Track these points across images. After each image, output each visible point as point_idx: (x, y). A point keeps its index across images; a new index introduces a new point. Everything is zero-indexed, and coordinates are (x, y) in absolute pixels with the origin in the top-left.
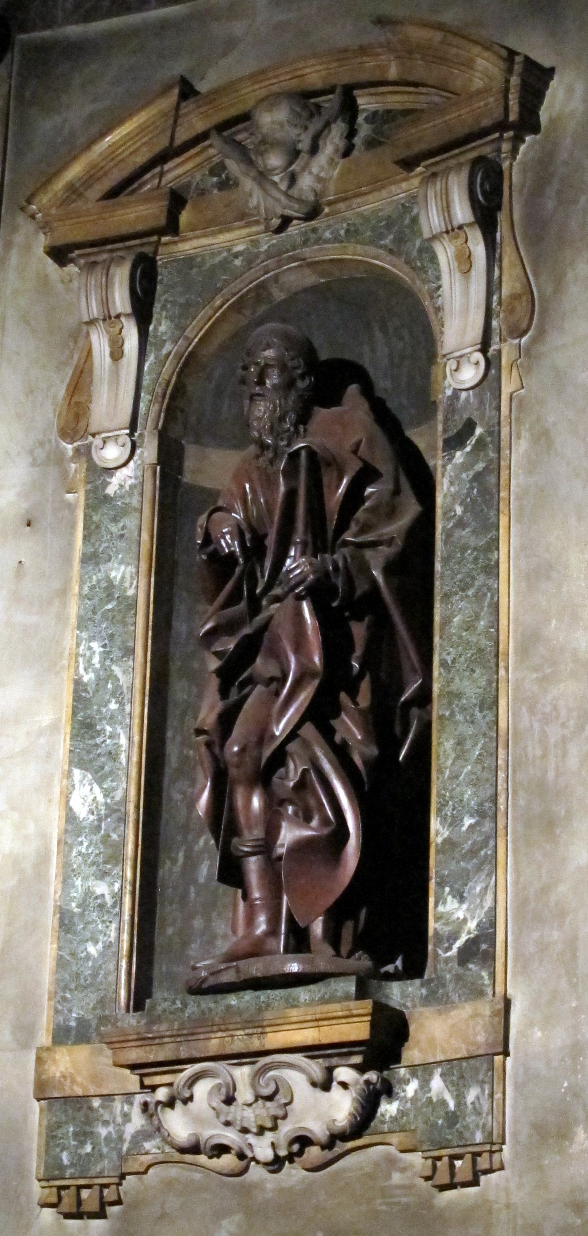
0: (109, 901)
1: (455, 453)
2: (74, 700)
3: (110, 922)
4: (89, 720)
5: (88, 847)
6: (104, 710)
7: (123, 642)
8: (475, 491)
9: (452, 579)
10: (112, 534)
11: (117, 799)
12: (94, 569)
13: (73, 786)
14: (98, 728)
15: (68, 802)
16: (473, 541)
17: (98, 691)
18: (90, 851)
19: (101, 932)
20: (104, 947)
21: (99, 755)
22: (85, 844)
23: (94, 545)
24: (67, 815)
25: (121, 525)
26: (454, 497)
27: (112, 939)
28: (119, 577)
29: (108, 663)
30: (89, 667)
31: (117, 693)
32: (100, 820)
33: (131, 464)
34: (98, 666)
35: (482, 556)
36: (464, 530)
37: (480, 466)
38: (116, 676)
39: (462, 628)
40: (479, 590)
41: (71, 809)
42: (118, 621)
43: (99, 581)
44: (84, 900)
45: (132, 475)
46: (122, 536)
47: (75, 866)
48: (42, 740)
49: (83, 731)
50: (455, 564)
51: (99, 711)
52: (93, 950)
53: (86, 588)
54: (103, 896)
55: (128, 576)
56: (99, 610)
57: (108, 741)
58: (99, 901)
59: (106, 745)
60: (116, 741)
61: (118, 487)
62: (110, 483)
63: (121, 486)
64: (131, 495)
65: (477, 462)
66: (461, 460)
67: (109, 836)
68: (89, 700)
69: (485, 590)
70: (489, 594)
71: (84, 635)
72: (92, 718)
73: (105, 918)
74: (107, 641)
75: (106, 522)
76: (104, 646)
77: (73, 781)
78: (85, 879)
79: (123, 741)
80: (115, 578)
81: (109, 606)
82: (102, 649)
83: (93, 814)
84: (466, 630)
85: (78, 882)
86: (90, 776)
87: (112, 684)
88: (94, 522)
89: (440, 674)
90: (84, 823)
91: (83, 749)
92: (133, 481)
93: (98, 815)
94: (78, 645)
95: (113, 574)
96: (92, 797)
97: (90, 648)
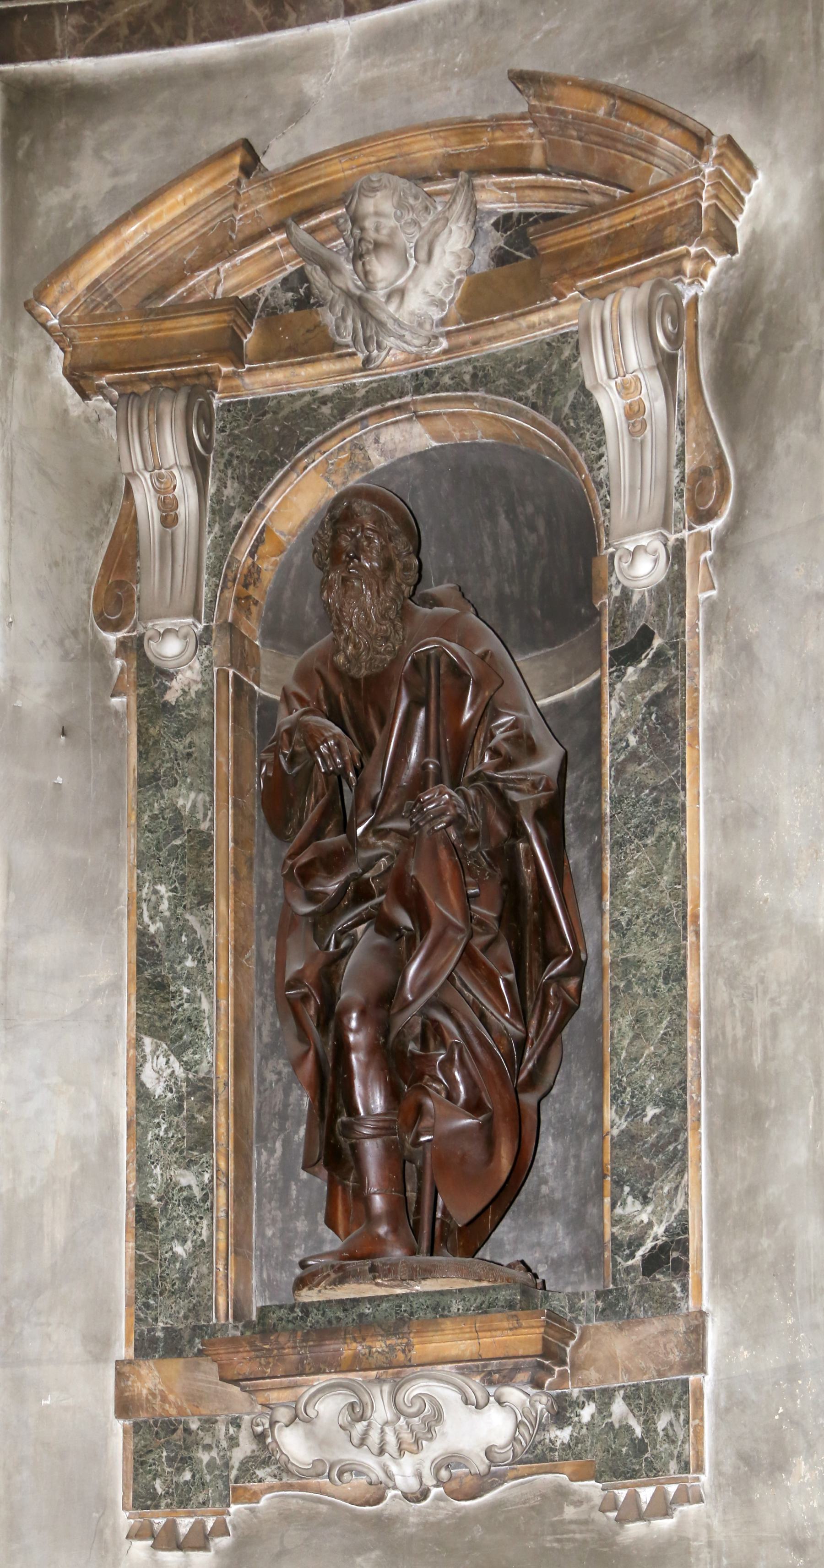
0: (197, 1193)
2: (138, 954)
3: (201, 1218)
4: (159, 979)
5: (166, 1131)
11: (201, 1075)
12: (155, 795)
13: (144, 1057)
14: (172, 989)
15: (138, 1076)
17: (168, 945)
18: (170, 1135)
19: (189, 1229)
21: (175, 1022)
22: (164, 1127)
23: (153, 765)
27: (204, 1237)
28: (188, 806)
29: (180, 910)
31: (195, 947)
32: (181, 1099)
34: (167, 914)
38: (192, 927)
41: (143, 1085)
43: (162, 810)
44: (166, 1192)
46: (189, 755)
51: (172, 967)
52: (179, 1249)
54: (190, 1187)
57: (186, 1005)
58: (185, 1194)
61: (180, 692)
64: (198, 704)
67: (193, 1117)
71: (147, 875)
73: (194, 1213)
76: (174, 890)
77: (143, 1050)
78: (166, 1167)
80: (184, 806)
81: (178, 842)
82: (171, 894)
85: (158, 1171)
87: (187, 936)
89: (612, 937)
90: (161, 1102)
91: (154, 1013)
93: (178, 1092)
94: (140, 887)
95: (181, 802)
96: (169, 1071)
97: (156, 892)
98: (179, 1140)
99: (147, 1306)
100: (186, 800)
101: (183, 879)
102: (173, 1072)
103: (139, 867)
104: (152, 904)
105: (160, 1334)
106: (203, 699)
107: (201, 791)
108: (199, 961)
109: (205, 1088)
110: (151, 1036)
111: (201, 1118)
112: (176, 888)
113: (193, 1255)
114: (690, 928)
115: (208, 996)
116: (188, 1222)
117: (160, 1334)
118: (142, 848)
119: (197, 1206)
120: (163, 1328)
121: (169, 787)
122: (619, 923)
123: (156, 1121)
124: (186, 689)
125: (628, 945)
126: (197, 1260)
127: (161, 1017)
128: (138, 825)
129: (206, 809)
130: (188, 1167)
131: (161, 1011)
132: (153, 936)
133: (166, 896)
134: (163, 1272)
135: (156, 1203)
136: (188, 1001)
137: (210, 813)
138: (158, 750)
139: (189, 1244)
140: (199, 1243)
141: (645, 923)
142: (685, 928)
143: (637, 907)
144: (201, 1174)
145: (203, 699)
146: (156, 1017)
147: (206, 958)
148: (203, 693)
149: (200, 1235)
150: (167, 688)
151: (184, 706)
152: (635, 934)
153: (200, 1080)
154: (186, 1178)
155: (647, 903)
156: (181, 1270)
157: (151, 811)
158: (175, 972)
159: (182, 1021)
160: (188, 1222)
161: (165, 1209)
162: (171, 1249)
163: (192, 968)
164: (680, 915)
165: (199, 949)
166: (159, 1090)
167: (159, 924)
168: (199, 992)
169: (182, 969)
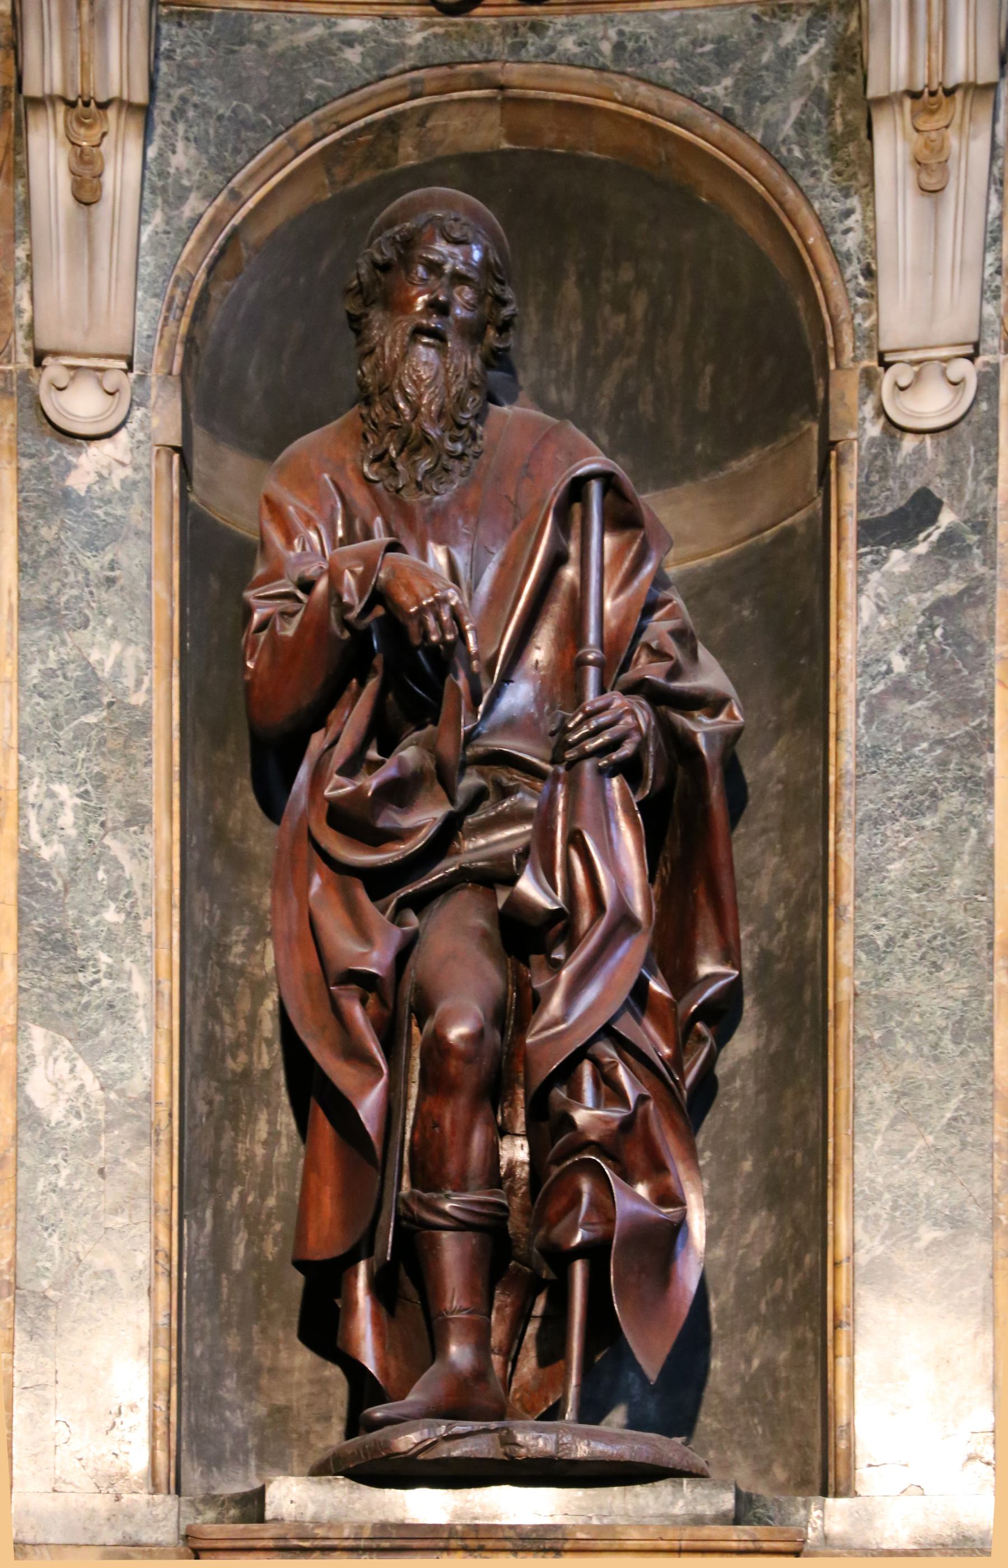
1: (888, 552)
2: (20, 891)
4: (58, 936)
6: (92, 921)
8: (939, 632)
9: (884, 791)
12: (50, 638)
13: (31, 1057)
14: (81, 953)
15: (18, 1086)
16: (932, 727)
18: (77, 1186)
21: (87, 1006)
22: (65, 1172)
25: (109, 557)
28: (109, 664)
29: (94, 829)
31: (117, 890)
32: (96, 1131)
33: (122, 435)
34: (72, 832)
35: (955, 757)
36: (911, 703)
37: (950, 587)
38: (115, 859)
39: (910, 886)
40: (947, 820)
41: (29, 1102)
42: (112, 752)
43: (63, 664)
45: (127, 459)
47: (44, 1212)
49: (45, 955)
50: (891, 762)
51: (79, 922)
53: (34, 673)
60: (124, 986)
61: (93, 478)
62: (76, 467)
64: (126, 501)
65: (946, 576)
66: (905, 568)
71: (37, 766)
72: (65, 932)
75: (72, 544)
76: (84, 795)
77: (29, 1046)
79: (139, 986)
80: (101, 663)
81: (91, 719)
82: (79, 801)
83: (78, 1115)
84: (919, 891)
85: (54, 1242)
86: (66, 1042)
87: (107, 872)
88: (43, 541)
89: (856, 961)
90: (59, 1133)
91: (50, 989)
92: (128, 472)
94: (22, 783)
95: (95, 656)
96: (76, 1084)
97: (51, 795)
100: (105, 654)
101: (100, 780)
102: (82, 1086)
103: (20, 750)
104: (45, 813)
106: (135, 494)
107: (129, 641)
108: (128, 914)
110: (42, 1025)
112: (86, 792)
118: (28, 720)
123: (52, 1161)
124: (105, 473)
125: (887, 976)
127: (62, 997)
128: (21, 682)
129: (141, 673)
131: (61, 988)
132: (47, 865)
136: (109, 975)
138: (55, 565)
141: (920, 946)
142: (991, 961)
143: (904, 920)
145: (135, 494)
146: (52, 996)
147: (140, 910)
148: (135, 483)
150: (69, 467)
151: (101, 500)
152: (901, 961)
155: (924, 915)
157: (43, 662)
159: (98, 1007)
163: (116, 924)
164: (984, 940)
165: (127, 896)
166: (56, 1113)
167: (58, 848)
168: (128, 964)
169: (98, 923)
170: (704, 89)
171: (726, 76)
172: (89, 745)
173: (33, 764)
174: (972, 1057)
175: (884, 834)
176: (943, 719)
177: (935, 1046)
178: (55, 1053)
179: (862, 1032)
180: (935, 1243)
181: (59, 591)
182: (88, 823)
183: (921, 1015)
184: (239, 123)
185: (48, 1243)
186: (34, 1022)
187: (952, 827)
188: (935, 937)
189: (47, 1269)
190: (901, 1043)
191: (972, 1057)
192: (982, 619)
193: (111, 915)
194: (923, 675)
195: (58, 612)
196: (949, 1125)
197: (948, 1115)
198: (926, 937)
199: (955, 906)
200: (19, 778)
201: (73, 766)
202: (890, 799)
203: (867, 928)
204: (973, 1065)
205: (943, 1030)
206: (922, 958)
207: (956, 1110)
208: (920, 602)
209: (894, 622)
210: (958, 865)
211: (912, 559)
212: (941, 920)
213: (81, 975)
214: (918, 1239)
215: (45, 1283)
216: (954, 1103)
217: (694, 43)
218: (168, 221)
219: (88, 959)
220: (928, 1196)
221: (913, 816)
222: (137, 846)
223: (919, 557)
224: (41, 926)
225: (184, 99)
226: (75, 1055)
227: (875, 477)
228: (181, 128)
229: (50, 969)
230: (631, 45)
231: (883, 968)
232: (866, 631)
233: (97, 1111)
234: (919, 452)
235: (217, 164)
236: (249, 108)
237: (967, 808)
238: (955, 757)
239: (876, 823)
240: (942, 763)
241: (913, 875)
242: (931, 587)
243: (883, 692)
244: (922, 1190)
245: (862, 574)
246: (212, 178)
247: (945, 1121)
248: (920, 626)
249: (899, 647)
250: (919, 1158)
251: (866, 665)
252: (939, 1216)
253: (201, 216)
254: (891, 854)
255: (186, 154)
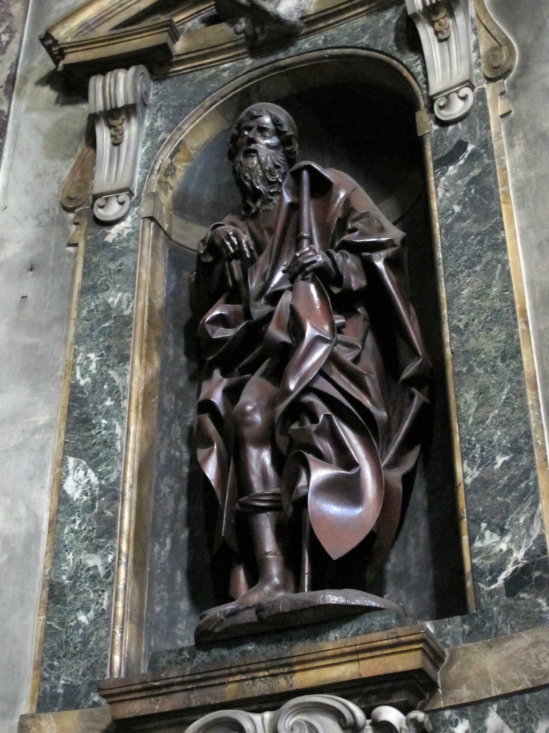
0: (102, 571)
3: (103, 591)
4: (84, 416)
5: (80, 525)
7: (119, 351)
8: (473, 191)
9: (456, 261)
10: (110, 270)
11: (112, 480)
12: (92, 298)
14: (94, 421)
17: (94, 392)
18: (83, 528)
19: (92, 601)
20: (95, 615)
21: (94, 445)
22: (78, 522)
23: (93, 279)
24: (60, 497)
25: (120, 262)
26: (451, 200)
27: (105, 607)
30: (86, 373)
32: (94, 500)
34: (94, 372)
35: (487, 238)
36: (464, 222)
39: (473, 298)
41: (64, 492)
42: (114, 336)
43: (97, 306)
44: (76, 572)
45: (130, 226)
46: (119, 271)
47: (67, 542)
48: (37, 436)
49: (78, 426)
51: (95, 408)
52: (83, 618)
53: (84, 312)
54: (96, 567)
55: (125, 302)
56: (97, 328)
57: (103, 432)
58: (91, 572)
59: (102, 436)
60: (112, 432)
61: (116, 235)
62: (109, 233)
63: (119, 235)
65: (473, 169)
67: (103, 513)
68: (86, 400)
69: (494, 263)
70: (499, 266)
71: (82, 348)
73: (98, 587)
74: (103, 352)
76: (102, 355)
77: (67, 467)
78: (78, 553)
80: (113, 302)
81: (107, 324)
82: (98, 358)
84: (477, 299)
85: (70, 557)
86: (84, 462)
87: (108, 385)
89: (452, 339)
90: (77, 504)
91: (78, 440)
92: (130, 230)
93: (92, 495)
95: (111, 300)
96: (86, 480)
97: (87, 358)
98: (89, 531)
99: (52, 667)
102: (89, 481)
105: (60, 691)
106: (132, 237)
107: (125, 291)
108: (116, 401)
109: (114, 490)
110: (75, 456)
111: (109, 513)
113: (94, 622)
114: (520, 320)
115: (121, 424)
116: (92, 595)
117: (60, 691)
119: (101, 582)
120: (64, 685)
121: (104, 291)
122: (458, 327)
123: (73, 518)
124: (121, 233)
126: (98, 626)
127: (84, 442)
129: (129, 301)
130: (95, 551)
132: (82, 387)
133: (95, 360)
134: (68, 637)
135: (67, 581)
136: (105, 429)
137: (131, 304)
139: (92, 614)
140: (100, 611)
141: (480, 323)
143: (472, 314)
144: (106, 556)
146: (79, 443)
149: (102, 605)
150: (107, 234)
153: (110, 485)
154: (94, 561)
156: (83, 635)
157: (89, 307)
158: (97, 410)
159: (99, 443)
160: (92, 595)
161: (73, 586)
162: (76, 618)
163: (110, 406)
166: (77, 496)
167: (88, 379)
168: (114, 422)
169: (103, 407)
170: (358, 42)
171: (366, 35)
172: (105, 335)
173: (81, 348)
174: (512, 367)
175: (459, 279)
176: (480, 224)
177: (493, 367)
178: (78, 468)
179: (457, 370)
180: (505, 462)
181: (98, 279)
182: (102, 366)
183: (485, 354)
184: (182, 106)
185: (68, 557)
186: (70, 455)
187: (489, 267)
188: (487, 317)
189: (66, 570)
190: (477, 370)
191: (512, 367)
192: (492, 180)
193: (109, 403)
194: (468, 209)
195: (97, 287)
196: (505, 402)
197: (504, 397)
198: (483, 318)
199: (495, 301)
200: (74, 355)
201: (97, 345)
202: (459, 264)
203: (455, 322)
204: (513, 370)
205: (495, 358)
206: (483, 327)
207: (507, 394)
208: (463, 182)
209: (453, 193)
210: (494, 282)
211: (458, 167)
212: (489, 308)
213: (93, 431)
214: (496, 464)
215: (64, 577)
216: (506, 390)
217: (353, 30)
218: (152, 144)
219: (97, 423)
220: (499, 440)
221: (470, 268)
222: (122, 371)
223: (461, 166)
224: (77, 413)
225: (161, 105)
226: (87, 467)
227: (439, 143)
228: (159, 114)
229: (79, 431)
230: (329, 39)
231: (464, 338)
232: (441, 201)
233: (95, 491)
234: (456, 129)
235: (171, 121)
236: (186, 101)
237: (495, 257)
238: (487, 238)
239: (454, 276)
240: (481, 242)
241: (473, 292)
242: (467, 175)
243: (452, 222)
244: (496, 438)
245: (437, 180)
246: (170, 126)
247: (502, 401)
248: (465, 191)
249: (456, 202)
250: (491, 422)
251: (442, 214)
252: (506, 449)
253: (165, 139)
254: (463, 287)
255: (161, 120)
